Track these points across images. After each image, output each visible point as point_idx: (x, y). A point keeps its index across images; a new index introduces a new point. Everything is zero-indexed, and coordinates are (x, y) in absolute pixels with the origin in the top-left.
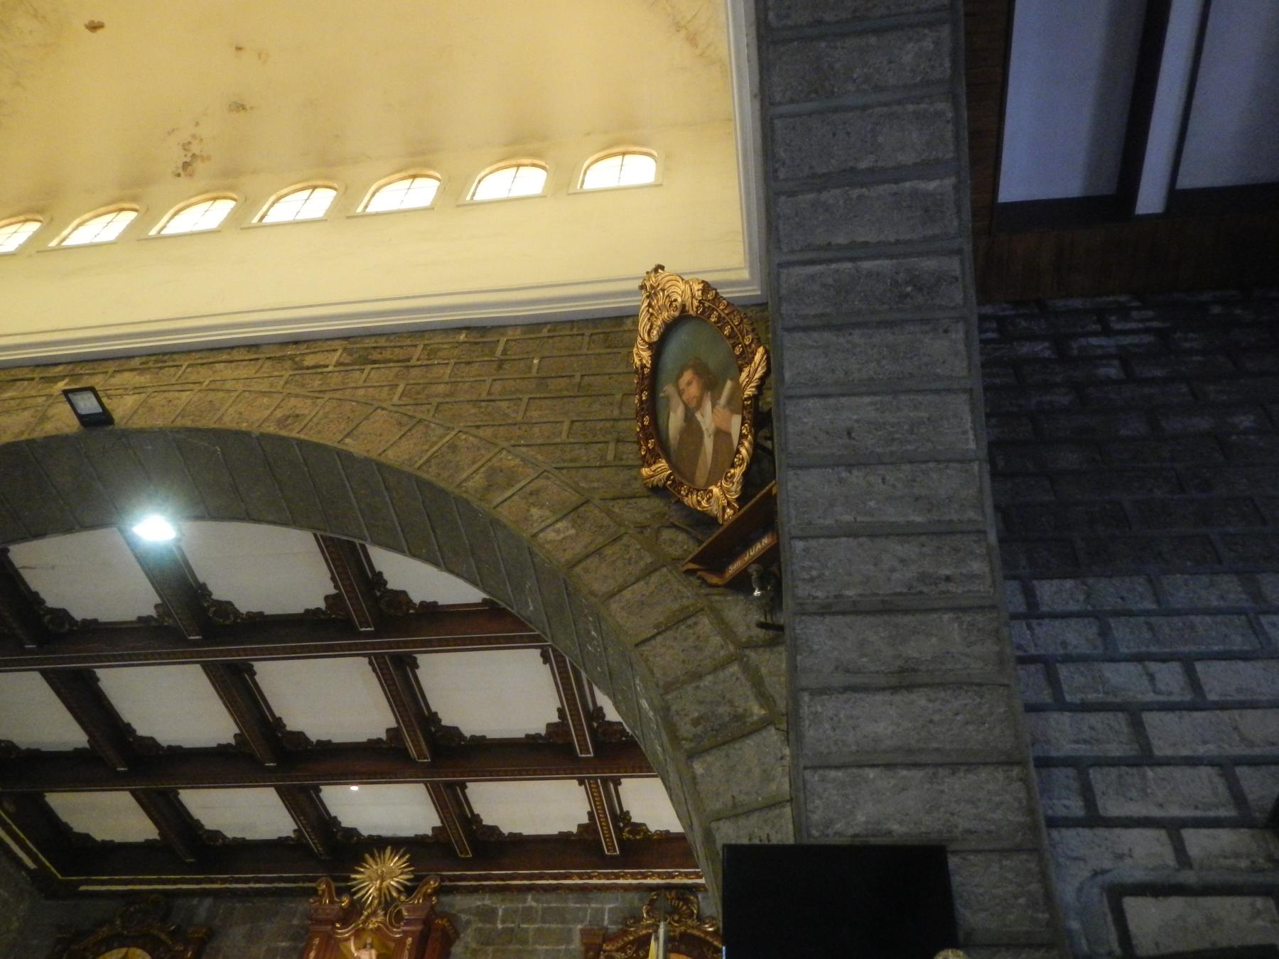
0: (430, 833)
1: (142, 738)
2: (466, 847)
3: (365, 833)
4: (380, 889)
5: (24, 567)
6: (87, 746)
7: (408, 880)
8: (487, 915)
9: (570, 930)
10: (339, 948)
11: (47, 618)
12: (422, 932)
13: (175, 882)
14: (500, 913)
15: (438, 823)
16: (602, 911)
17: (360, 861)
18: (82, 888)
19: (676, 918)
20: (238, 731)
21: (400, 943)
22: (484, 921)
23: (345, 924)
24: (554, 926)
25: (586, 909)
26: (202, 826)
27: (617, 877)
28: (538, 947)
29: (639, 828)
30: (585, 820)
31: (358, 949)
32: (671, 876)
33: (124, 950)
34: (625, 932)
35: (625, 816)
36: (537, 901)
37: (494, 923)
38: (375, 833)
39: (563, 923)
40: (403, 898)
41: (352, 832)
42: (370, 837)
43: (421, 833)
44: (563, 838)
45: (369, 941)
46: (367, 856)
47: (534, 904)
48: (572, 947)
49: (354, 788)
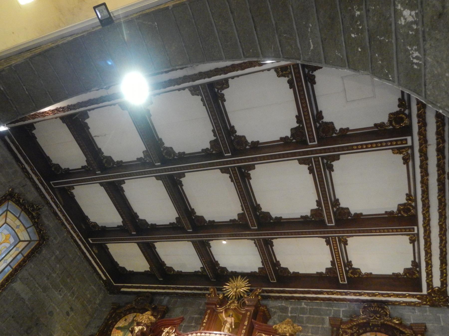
0: (257, 270)
1: (142, 220)
2: (273, 275)
3: (230, 270)
4: (236, 292)
5: (95, 136)
6: (122, 224)
7: (248, 289)
8: (284, 310)
9: (323, 319)
11: (105, 160)
13: (155, 288)
14: (290, 309)
15: (261, 266)
16: (340, 310)
17: (228, 281)
18: (122, 290)
19: (378, 316)
20: (178, 216)
21: (244, 315)
22: (282, 312)
23: (221, 306)
25: (331, 310)
26: (165, 264)
27: (346, 294)
28: (308, 325)
29: (356, 271)
30: (329, 266)
31: (226, 317)
32: (374, 295)
33: (135, 314)
34: (352, 321)
35: (349, 264)
36: (307, 305)
37: (288, 313)
38: (234, 270)
40: (246, 296)
41: (224, 269)
42: (232, 272)
43: (253, 271)
44: (319, 276)
45: (231, 314)
46: (230, 279)
47: (305, 306)
48: (325, 326)
49: (224, 242)
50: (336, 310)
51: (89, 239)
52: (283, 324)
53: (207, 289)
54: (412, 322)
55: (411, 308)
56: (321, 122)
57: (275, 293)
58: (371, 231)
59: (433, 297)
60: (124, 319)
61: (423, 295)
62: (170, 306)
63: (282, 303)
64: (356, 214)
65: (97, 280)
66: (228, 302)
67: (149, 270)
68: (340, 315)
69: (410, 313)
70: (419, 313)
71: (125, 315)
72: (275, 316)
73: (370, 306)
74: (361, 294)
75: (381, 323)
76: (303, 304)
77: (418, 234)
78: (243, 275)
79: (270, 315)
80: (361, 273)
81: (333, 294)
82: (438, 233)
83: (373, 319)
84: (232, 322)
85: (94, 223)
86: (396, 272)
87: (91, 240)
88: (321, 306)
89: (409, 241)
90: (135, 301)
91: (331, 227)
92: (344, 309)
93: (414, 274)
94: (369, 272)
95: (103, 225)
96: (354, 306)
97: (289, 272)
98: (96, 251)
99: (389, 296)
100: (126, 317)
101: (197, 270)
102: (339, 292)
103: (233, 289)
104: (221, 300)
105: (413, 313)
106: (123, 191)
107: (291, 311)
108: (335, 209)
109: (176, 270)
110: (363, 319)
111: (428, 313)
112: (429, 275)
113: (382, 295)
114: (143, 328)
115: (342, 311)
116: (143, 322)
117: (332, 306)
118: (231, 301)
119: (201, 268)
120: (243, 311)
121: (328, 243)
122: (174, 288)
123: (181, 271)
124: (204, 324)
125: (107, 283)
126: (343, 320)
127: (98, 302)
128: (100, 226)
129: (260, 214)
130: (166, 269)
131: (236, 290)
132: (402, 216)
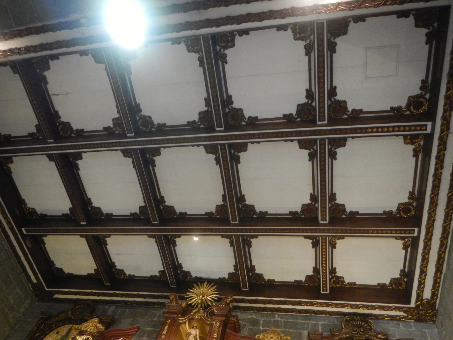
0: (227, 276)
2: (245, 283)
3: (194, 275)
5: (54, 95)
7: (216, 297)
8: (255, 323)
9: (300, 333)
10: (178, 327)
12: (224, 321)
13: (99, 295)
14: (261, 322)
16: (319, 324)
17: (192, 287)
18: (56, 296)
19: (362, 330)
22: (253, 325)
23: (183, 316)
24: (291, 330)
25: (308, 324)
26: (116, 266)
27: (328, 305)
29: (339, 280)
31: (190, 328)
32: (357, 307)
33: (71, 325)
35: (333, 271)
36: (281, 318)
38: (198, 275)
39: (296, 329)
40: (214, 304)
41: (188, 273)
42: (196, 278)
43: (222, 277)
45: (195, 325)
46: (195, 285)
47: (279, 319)
49: (196, 239)
50: (315, 324)
51: (23, 229)
52: (268, 333)
53: (167, 297)
54: (398, 338)
55: (395, 322)
56: (333, 100)
57: (246, 303)
58: (368, 232)
59: (421, 310)
60: (55, 331)
61: (410, 308)
62: (116, 317)
63: (252, 315)
64: (351, 212)
65: (25, 283)
66: (192, 312)
67: (93, 272)
68: (319, 330)
69: (395, 329)
70: (404, 329)
71: (57, 327)
72: (245, 329)
73: (353, 320)
74: (343, 306)
75: (366, 338)
76: (277, 316)
77: (418, 237)
78: (210, 281)
79: (239, 328)
80: (344, 282)
81: (312, 304)
82: (440, 236)
83: (357, 334)
84: (196, 335)
85: (31, 209)
86: (382, 282)
87: (25, 230)
88: (297, 319)
89: (402, 246)
90: (71, 309)
91: (324, 225)
92: (323, 323)
93: (401, 285)
94: (352, 281)
95: (44, 213)
96: (334, 320)
97: (263, 279)
98: (30, 246)
99: (374, 308)
100: (59, 329)
101: (154, 274)
102: (320, 303)
103: (197, 296)
104: (183, 309)
105: (398, 328)
106: (78, 169)
107: (263, 324)
108: (330, 205)
109: (128, 273)
110: (346, 333)
111: (413, 329)
112: (421, 284)
113: (366, 307)
114: (88, 338)
115: (321, 325)
116: (89, 330)
117: (309, 320)
118: (196, 310)
119: (160, 271)
120: (210, 321)
121: (315, 245)
122: (122, 295)
123: (134, 275)
124: (163, 337)
125: (37, 287)
126: (324, 335)
127: (22, 310)
128: (39, 213)
129: (242, 208)
130: (115, 273)
131: (203, 296)
132: (401, 217)
